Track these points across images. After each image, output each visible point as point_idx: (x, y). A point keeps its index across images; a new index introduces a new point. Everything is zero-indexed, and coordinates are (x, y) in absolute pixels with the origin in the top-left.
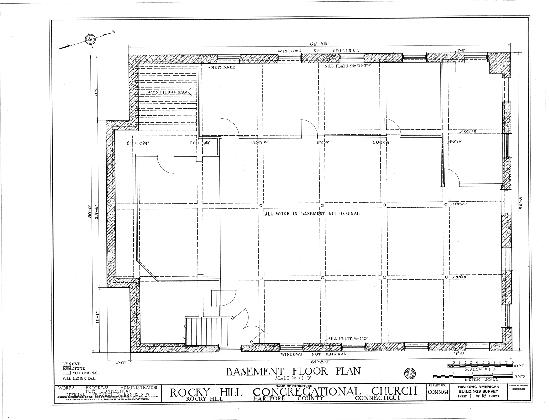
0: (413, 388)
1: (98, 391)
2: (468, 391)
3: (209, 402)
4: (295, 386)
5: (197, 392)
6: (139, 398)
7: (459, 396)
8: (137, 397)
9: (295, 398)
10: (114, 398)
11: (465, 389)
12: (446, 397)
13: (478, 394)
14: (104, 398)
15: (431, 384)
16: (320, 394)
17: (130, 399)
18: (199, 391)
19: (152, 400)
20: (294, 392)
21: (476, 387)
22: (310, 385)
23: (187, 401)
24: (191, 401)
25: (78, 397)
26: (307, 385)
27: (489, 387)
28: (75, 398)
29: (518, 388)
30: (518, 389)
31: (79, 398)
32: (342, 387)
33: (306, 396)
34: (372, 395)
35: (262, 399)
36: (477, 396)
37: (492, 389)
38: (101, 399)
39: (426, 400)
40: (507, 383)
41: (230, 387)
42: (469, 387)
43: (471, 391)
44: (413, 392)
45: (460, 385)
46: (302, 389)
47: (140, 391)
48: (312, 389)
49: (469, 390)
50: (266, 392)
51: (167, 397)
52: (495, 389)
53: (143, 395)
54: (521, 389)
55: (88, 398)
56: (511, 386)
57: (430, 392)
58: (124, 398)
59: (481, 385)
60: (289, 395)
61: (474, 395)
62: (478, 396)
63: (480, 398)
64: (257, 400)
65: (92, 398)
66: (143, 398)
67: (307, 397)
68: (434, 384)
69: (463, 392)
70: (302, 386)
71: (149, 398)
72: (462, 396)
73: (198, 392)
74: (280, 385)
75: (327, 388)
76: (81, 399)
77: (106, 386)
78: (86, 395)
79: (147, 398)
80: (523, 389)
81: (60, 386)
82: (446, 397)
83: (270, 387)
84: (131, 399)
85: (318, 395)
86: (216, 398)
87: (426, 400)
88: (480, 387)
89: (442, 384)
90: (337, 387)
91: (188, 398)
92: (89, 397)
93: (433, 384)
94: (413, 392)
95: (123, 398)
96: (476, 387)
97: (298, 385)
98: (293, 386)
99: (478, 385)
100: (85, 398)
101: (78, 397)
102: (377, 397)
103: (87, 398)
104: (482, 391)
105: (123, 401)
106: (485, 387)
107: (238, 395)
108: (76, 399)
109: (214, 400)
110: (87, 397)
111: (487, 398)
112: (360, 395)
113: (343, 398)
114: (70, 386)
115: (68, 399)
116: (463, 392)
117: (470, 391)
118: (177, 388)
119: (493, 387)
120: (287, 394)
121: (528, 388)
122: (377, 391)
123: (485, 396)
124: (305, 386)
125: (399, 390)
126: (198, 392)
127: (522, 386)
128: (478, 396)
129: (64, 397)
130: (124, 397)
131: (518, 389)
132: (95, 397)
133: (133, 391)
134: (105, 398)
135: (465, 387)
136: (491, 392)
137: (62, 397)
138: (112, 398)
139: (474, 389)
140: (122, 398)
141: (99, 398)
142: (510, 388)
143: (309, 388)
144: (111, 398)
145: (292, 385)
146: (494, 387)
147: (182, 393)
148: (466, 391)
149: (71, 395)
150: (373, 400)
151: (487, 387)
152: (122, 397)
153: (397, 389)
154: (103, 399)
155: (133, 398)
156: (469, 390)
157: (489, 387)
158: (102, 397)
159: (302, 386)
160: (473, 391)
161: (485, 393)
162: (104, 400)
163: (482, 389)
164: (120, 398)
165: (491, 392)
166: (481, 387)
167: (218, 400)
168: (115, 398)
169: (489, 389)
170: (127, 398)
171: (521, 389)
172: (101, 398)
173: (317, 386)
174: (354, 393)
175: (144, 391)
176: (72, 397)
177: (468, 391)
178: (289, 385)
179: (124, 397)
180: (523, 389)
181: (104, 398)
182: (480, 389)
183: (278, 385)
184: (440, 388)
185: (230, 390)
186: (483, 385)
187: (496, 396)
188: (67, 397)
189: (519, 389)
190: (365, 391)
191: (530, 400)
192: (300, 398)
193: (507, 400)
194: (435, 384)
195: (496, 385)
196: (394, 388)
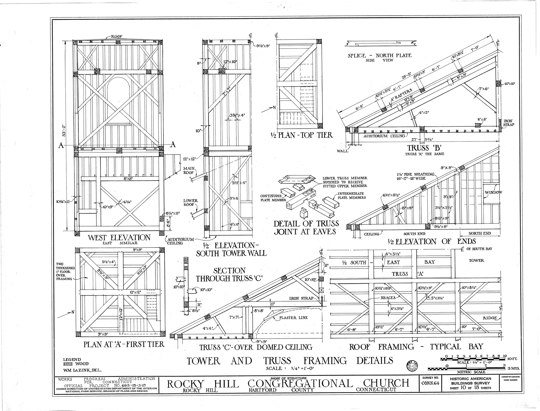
0: (405, 380)
2: (460, 383)
5: (192, 384)
7: (451, 388)
9: (289, 390)
10: (113, 390)
11: (457, 381)
12: (437, 388)
13: (470, 386)
14: (104, 390)
18: (194, 383)
19: (150, 391)
20: (288, 383)
21: (468, 379)
22: (304, 377)
23: (183, 392)
25: (78, 389)
31: (78, 390)
32: (334, 378)
36: (469, 388)
37: (483, 381)
39: (442, 391)
40: (499, 374)
42: (461, 379)
43: (463, 383)
44: (405, 384)
46: (295, 380)
47: (137, 382)
49: (461, 382)
51: (164, 388)
52: (487, 381)
54: (513, 380)
55: (88, 390)
56: (504, 377)
61: (467, 386)
63: (473, 389)
65: (92, 390)
67: (300, 389)
69: (455, 384)
72: (454, 388)
76: (80, 391)
80: (515, 380)
82: (437, 388)
83: (263, 379)
84: (130, 391)
85: (310, 387)
86: (211, 389)
87: (442, 391)
91: (184, 390)
94: (405, 384)
96: (468, 379)
100: (85, 390)
101: (78, 389)
103: (86, 390)
104: (473, 383)
105: (122, 393)
108: (76, 390)
109: (209, 392)
110: (87, 389)
111: (480, 390)
113: (335, 389)
116: (455, 384)
117: (462, 383)
119: (485, 379)
123: (478, 388)
131: (509, 380)
134: (105, 390)
135: (457, 379)
136: (482, 383)
138: (111, 390)
139: (466, 381)
141: (98, 390)
142: (502, 379)
143: (301, 380)
144: (110, 390)
147: (178, 384)
148: (458, 383)
156: (461, 382)
160: (465, 383)
161: (477, 385)
162: (103, 391)
163: (473, 381)
164: (119, 390)
165: (482, 383)
167: (213, 391)
168: (114, 390)
169: (481, 381)
170: (126, 390)
171: (513, 380)
177: (460, 383)
180: (515, 380)
181: (104, 390)
182: (472, 381)
187: (488, 388)
192: (294, 390)
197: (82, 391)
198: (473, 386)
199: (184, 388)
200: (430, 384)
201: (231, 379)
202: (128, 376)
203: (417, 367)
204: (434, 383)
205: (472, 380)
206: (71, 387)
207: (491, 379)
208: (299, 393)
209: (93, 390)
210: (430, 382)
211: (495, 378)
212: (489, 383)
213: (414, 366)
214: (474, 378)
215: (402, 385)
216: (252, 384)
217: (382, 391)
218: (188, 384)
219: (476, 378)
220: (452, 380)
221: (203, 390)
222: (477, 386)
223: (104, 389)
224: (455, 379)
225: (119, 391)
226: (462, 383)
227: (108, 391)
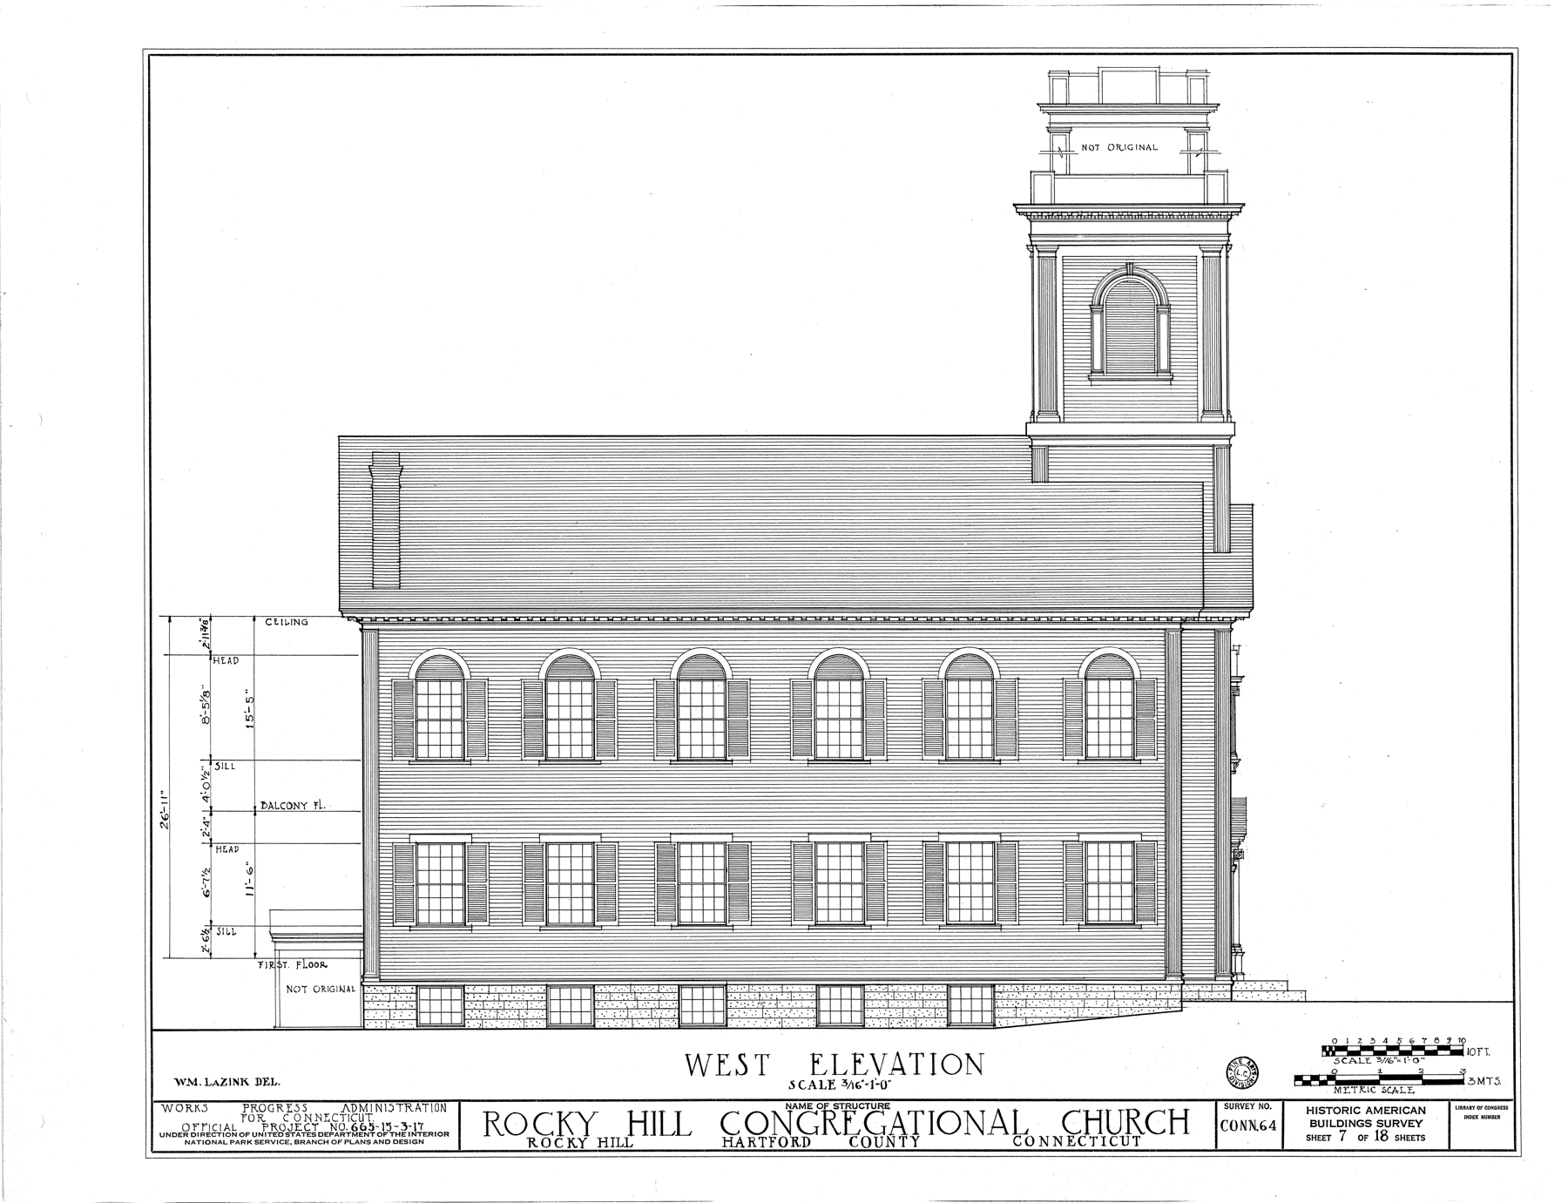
0: (1179, 1113)
2: (1334, 1123)
3: (596, 1151)
4: (840, 1106)
5: (560, 1121)
6: (394, 1138)
7: (1309, 1138)
8: (388, 1136)
10: (324, 1138)
11: (1326, 1117)
12: (1271, 1139)
13: (1364, 1131)
15: (1229, 1102)
16: (910, 1130)
17: (369, 1142)
19: (430, 1143)
20: (839, 1122)
21: (1357, 1110)
22: (884, 1104)
24: (540, 1148)
25: (221, 1135)
26: (874, 1102)
27: (1394, 1110)
28: (211, 1139)
30: (1480, 1117)
31: (221, 1138)
32: (974, 1108)
33: (872, 1137)
34: (1061, 1132)
35: (746, 1143)
36: (1361, 1138)
40: (1449, 1101)
41: (658, 1107)
42: (1337, 1110)
43: (1344, 1123)
44: (1179, 1125)
45: (1311, 1105)
46: (861, 1114)
47: (398, 1116)
48: (888, 1118)
49: (1338, 1121)
50: (757, 1124)
52: (1413, 1116)
53: (376, 1130)
54: (1489, 1117)
55: (250, 1137)
56: (1461, 1108)
57: (1226, 1126)
58: (350, 1138)
60: (825, 1133)
61: (1353, 1132)
62: (1362, 1138)
63: (1371, 1143)
64: (733, 1147)
66: (407, 1138)
67: (876, 1138)
68: (1239, 1102)
69: (1321, 1124)
70: (862, 1106)
71: (422, 1138)
72: (1317, 1138)
73: (563, 1123)
74: (797, 1103)
75: (932, 1112)
76: (227, 1140)
77: (301, 1104)
78: (240, 1128)
79: (418, 1138)
80: (1493, 1117)
81: (165, 1104)
82: (1271, 1139)
83: (767, 1108)
84: (372, 1142)
85: (905, 1133)
86: (616, 1140)
88: (1369, 1110)
89: (1261, 1102)
90: (960, 1107)
91: (531, 1141)
92: (251, 1134)
93: (1235, 1102)
94: (1179, 1125)
95: (349, 1138)
96: (1357, 1110)
97: (849, 1105)
99: (1364, 1106)
100: (240, 1139)
101: (221, 1135)
102: (1075, 1140)
103: (244, 1138)
104: (1374, 1123)
105: (348, 1147)
106: (1385, 1110)
107: (678, 1134)
108: (214, 1139)
109: (608, 1147)
110: (247, 1134)
111: (1391, 1143)
112: (1026, 1133)
113: (977, 1140)
114: (197, 1104)
115: (191, 1139)
116: (1321, 1124)
117: (1340, 1124)
118: (503, 1109)
119: (1406, 1110)
120: (821, 1130)
121: (1507, 1115)
122: (1075, 1123)
124: (870, 1106)
125: (497, 1119)
128: (1362, 1138)
129: (179, 1135)
130: (351, 1135)
131: (1480, 1117)
132: (268, 1135)
133: (379, 1118)
134: (298, 1138)
135: (1327, 1110)
136: (1400, 1124)
137: (173, 1135)
138: (317, 1138)
139: (1353, 1117)
140: (346, 1137)
141: (279, 1139)
142: (1458, 1115)
143: (883, 1112)
144: (315, 1139)
145: (832, 1103)
146: (1410, 1111)
147: (516, 1124)
148: (1328, 1124)
149: (199, 1129)
150: (1065, 1146)
151: (1390, 1111)
152: (346, 1135)
153: (1133, 1114)
154: (292, 1139)
156: (1338, 1121)
157: (1394, 1110)
158: (288, 1135)
159: (862, 1106)
160: (1350, 1121)
161: (1384, 1128)
163: (1374, 1118)
164: (340, 1138)
165: (1400, 1124)
166: (1373, 1110)
167: (620, 1145)
168: (326, 1139)
169: (1394, 1116)
170: (359, 1139)
171: (1489, 1117)
172: (284, 1138)
173: (903, 1107)
174: (1010, 1129)
175: (411, 1117)
176: (202, 1134)
177: (1334, 1123)
178: (823, 1102)
179: (351, 1135)
180: (1493, 1117)
182: (1369, 1116)
183: (791, 1104)
184: (1256, 1114)
185: (658, 1116)
186: (1379, 1105)
187: (1416, 1138)
188: (189, 1135)
189: (1483, 1117)
190: (1042, 1122)
191: (1515, 1150)
192: (856, 1142)
193: (1281, 1148)
194: (1242, 1102)
195: (1417, 1105)
196: (1124, 1114)
197: (231, 1142)
198: (1370, 1132)
199: (534, 1135)
202: (372, 1101)
204: (1261, 1127)
205: (1369, 1113)
207: (1424, 1113)
209: (264, 1138)
210: (1248, 1123)
212: (1419, 1124)
214: (1375, 1108)
215: (1168, 1131)
216: (734, 1124)
217: (1104, 1145)
218: (549, 1124)
219: (1381, 1108)
221: (591, 1143)
222: (1384, 1132)
223: (295, 1135)
224: (1322, 1111)
226: (1341, 1124)
227: (309, 1142)
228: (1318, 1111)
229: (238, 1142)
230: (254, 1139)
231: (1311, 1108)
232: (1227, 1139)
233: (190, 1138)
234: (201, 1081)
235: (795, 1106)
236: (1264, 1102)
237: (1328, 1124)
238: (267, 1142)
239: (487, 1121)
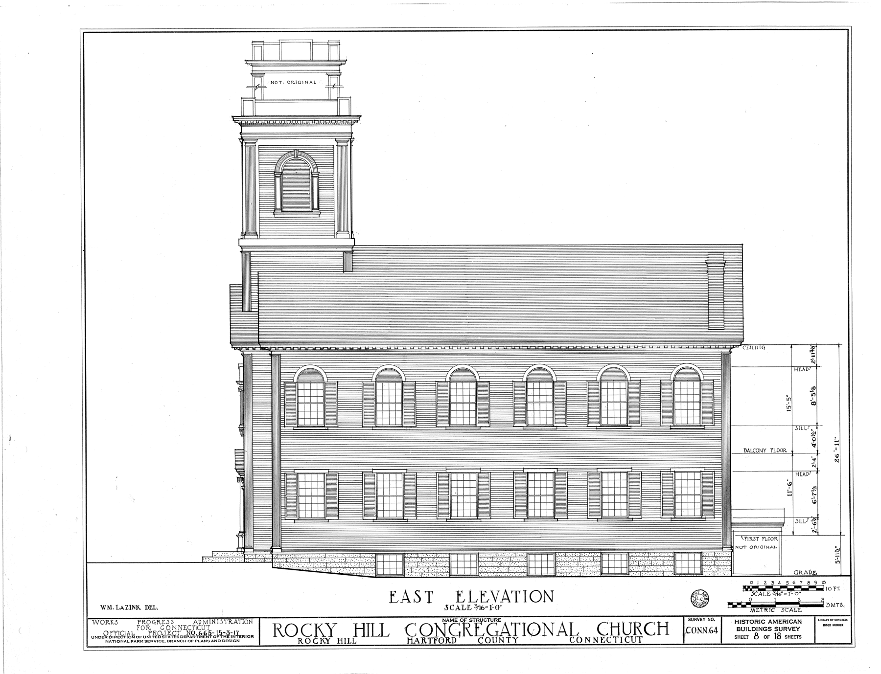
1: (156, 627)
2: (750, 629)
4: (473, 620)
5: (316, 628)
6: (223, 638)
7: (736, 637)
10: (183, 639)
11: (746, 625)
12: (715, 638)
13: (767, 633)
14: (167, 639)
16: (512, 633)
18: (318, 627)
19: (243, 641)
21: (763, 622)
22: (498, 619)
24: (305, 644)
26: (492, 618)
27: (784, 621)
28: (120, 639)
29: (832, 623)
31: (126, 639)
32: (548, 621)
33: (491, 637)
37: (789, 625)
38: (162, 641)
40: (815, 616)
42: (752, 622)
43: (756, 629)
44: (663, 630)
46: (485, 624)
47: (225, 627)
48: (499, 627)
52: (795, 625)
54: (837, 625)
55: (142, 639)
56: (821, 620)
58: (198, 639)
59: (772, 618)
61: (761, 634)
62: (767, 637)
63: (772, 640)
64: (411, 643)
65: (148, 639)
68: (696, 617)
69: (743, 630)
71: (238, 638)
72: (741, 637)
74: (449, 618)
76: (129, 640)
79: (236, 638)
80: (839, 625)
82: (715, 638)
83: (432, 621)
84: (211, 641)
88: (770, 621)
89: (709, 617)
90: (540, 621)
91: (300, 640)
92: (142, 637)
94: (663, 630)
96: (763, 622)
98: (471, 621)
100: (136, 639)
103: (139, 639)
104: (773, 629)
105: (197, 644)
108: (122, 640)
110: (140, 637)
111: (783, 640)
113: (549, 639)
115: (109, 640)
116: (743, 630)
117: (754, 629)
119: (791, 622)
120: (462, 634)
122: (605, 629)
124: (490, 620)
126: (318, 629)
127: (839, 620)
128: (767, 637)
131: (832, 625)
134: (169, 639)
135: (746, 622)
136: (788, 629)
137: (99, 637)
138: (180, 639)
139: (761, 625)
140: (196, 638)
141: (159, 639)
142: (819, 624)
144: (178, 639)
145: (468, 619)
147: (291, 630)
148: (747, 629)
151: (782, 622)
152: (196, 637)
153: (637, 625)
154: (165, 640)
155: (214, 639)
157: (784, 621)
159: (485, 620)
161: (779, 631)
162: (166, 641)
163: (773, 626)
164: (192, 639)
165: (788, 629)
167: (350, 642)
168: (185, 639)
169: (784, 625)
170: (203, 639)
171: (837, 625)
172: (161, 639)
173: (508, 621)
174: (568, 633)
177: (750, 629)
178: (463, 618)
180: (839, 625)
181: (167, 639)
182: (770, 625)
184: (706, 624)
187: (796, 637)
190: (586, 629)
194: (698, 617)
195: (797, 618)
196: (633, 624)
200: (702, 629)
201: (377, 622)
203: (707, 601)
206: (117, 634)
207: (801, 623)
208: (305, 646)
211: (808, 622)
212: (798, 629)
213: (703, 599)
214: (774, 620)
218: (309, 631)
219: (777, 620)
220: (737, 623)
221: (333, 641)
224: (743, 622)
225: (192, 641)
228: (741, 622)
229: (135, 641)
230: (144, 639)
231: (737, 621)
232: (689, 638)
233: (108, 639)
234: (114, 607)
235: (448, 620)
236: (711, 617)
237: (747, 629)
238: (152, 641)
239: (275, 629)
